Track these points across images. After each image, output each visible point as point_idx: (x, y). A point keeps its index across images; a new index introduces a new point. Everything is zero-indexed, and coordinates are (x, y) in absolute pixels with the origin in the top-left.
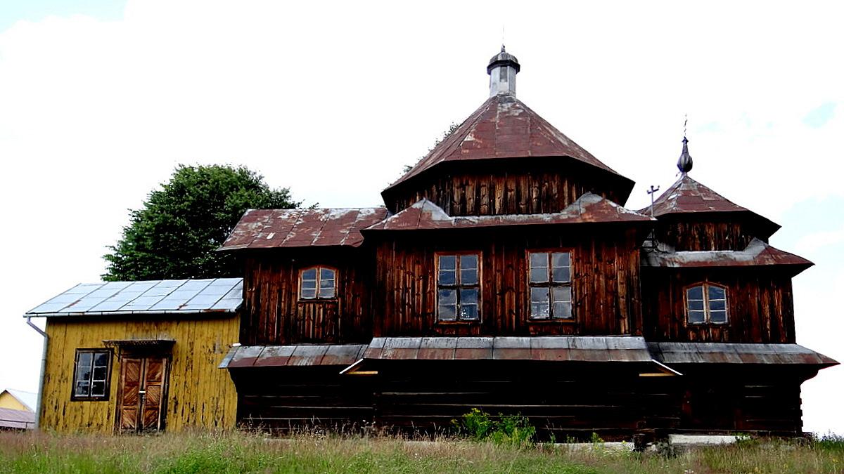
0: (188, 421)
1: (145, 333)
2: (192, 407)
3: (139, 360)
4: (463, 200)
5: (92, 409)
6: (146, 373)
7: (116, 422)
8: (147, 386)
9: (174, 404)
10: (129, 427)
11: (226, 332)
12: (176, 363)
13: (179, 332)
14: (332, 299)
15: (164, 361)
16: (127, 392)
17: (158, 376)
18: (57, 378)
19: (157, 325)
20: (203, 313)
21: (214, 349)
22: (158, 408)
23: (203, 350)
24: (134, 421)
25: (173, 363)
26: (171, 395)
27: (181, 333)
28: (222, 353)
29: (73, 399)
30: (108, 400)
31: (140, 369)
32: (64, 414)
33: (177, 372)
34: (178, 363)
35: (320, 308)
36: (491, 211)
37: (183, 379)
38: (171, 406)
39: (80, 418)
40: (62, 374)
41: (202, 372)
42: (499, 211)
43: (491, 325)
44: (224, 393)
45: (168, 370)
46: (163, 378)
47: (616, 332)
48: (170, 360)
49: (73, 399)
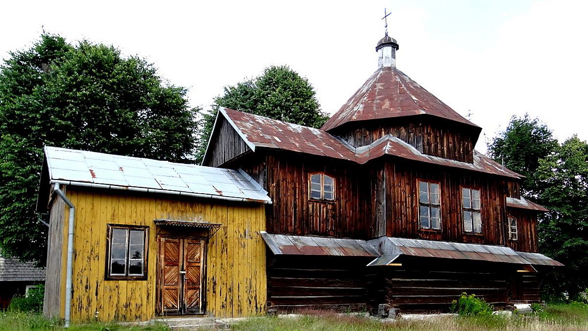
0: (226, 300)
1: (180, 215)
2: (228, 287)
3: (177, 240)
5: (129, 290)
6: (185, 254)
7: (156, 302)
8: (187, 267)
9: (212, 284)
10: (171, 306)
11: (253, 220)
12: (212, 246)
13: (213, 215)
14: (333, 201)
15: (202, 243)
16: (168, 272)
17: (197, 256)
18: (86, 255)
19: (192, 207)
20: (245, 201)
21: (245, 235)
22: (199, 288)
23: (235, 234)
24: (176, 301)
25: (209, 245)
27: (215, 218)
28: (252, 238)
29: (107, 278)
31: (179, 250)
32: (97, 294)
33: (214, 254)
34: (214, 245)
35: (323, 208)
36: (443, 157)
38: (210, 286)
40: (92, 251)
41: (236, 256)
44: (255, 275)
45: (206, 251)
46: (202, 259)
48: (207, 242)
49: (107, 278)
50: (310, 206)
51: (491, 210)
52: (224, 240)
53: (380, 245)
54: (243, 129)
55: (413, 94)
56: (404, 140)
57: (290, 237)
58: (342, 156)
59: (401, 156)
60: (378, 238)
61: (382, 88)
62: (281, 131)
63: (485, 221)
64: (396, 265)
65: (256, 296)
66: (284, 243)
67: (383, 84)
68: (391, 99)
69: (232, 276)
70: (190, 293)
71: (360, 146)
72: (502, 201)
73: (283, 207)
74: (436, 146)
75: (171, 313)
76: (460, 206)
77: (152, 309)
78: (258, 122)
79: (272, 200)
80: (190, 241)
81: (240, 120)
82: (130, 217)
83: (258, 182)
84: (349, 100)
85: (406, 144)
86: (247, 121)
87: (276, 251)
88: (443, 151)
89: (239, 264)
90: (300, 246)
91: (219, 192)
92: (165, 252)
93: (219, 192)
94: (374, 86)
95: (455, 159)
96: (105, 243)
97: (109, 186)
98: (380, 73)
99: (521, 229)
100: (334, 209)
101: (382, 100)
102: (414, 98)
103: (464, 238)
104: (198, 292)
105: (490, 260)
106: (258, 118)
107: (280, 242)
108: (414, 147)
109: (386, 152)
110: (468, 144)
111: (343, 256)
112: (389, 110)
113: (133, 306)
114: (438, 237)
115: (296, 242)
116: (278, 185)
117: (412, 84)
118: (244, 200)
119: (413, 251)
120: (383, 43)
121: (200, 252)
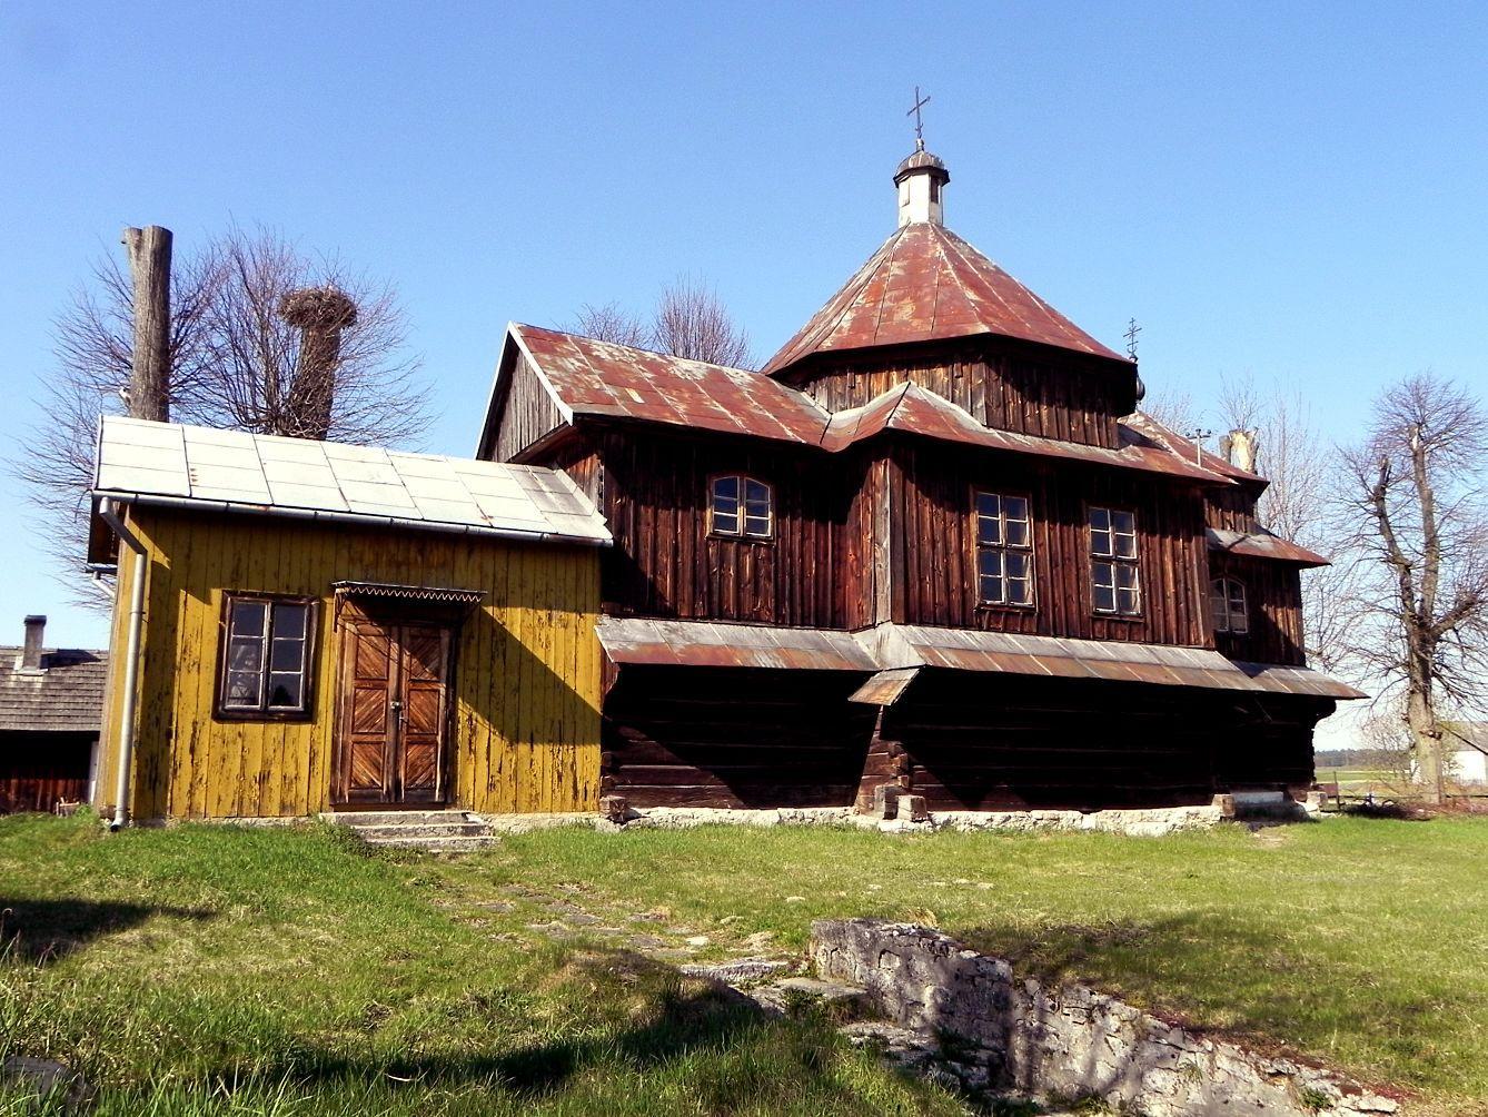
1: (394, 571)
11: (571, 583)
13: (473, 571)
14: (766, 539)
15: (445, 638)
28: (565, 627)
32: (192, 750)
33: (473, 663)
34: (474, 642)
37: (485, 677)
39: (239, 760)
42: (1049, 429)
47: (1184, 641)
48: (455, 637)
49: (220, 715)
53: (879, 646)
54: (555, 373)
56: (942, 394)
58: (790, 433)
59: (926, 432)
60: (874, 626)
61: (897, 272)
62: (650, 375)
65: (574, 762)
66: (639, 637)
67: (905, 263)
68: (916, 300)
70: (413, 752)
71: (842, 409)
75: (365, 799)
77: (321, 787)
78: (597, 356)
80: (414, 631)
82: (277, 575)
84: (829, 302)
85: (948, 403)
86: (572, 354)
91: (485, 518)
93: (485, 518)
94: (883, 269)
96: (215, 633)
97: (225, 504)
98: (901, 239)
101: (897, 299)
104: (432, 750)
106: (600, 348)
107: (632, 636)
108: (966, 410)
109: (890, 424)
111: (783, 670)
112: (909, 322)
113: (275, 781)
114: (1032, 624)
115: (673, 636)
117: (974, 262)
118: (545, 535)
119: (954, 658)
120: (911, 166)
121: (440, 656)
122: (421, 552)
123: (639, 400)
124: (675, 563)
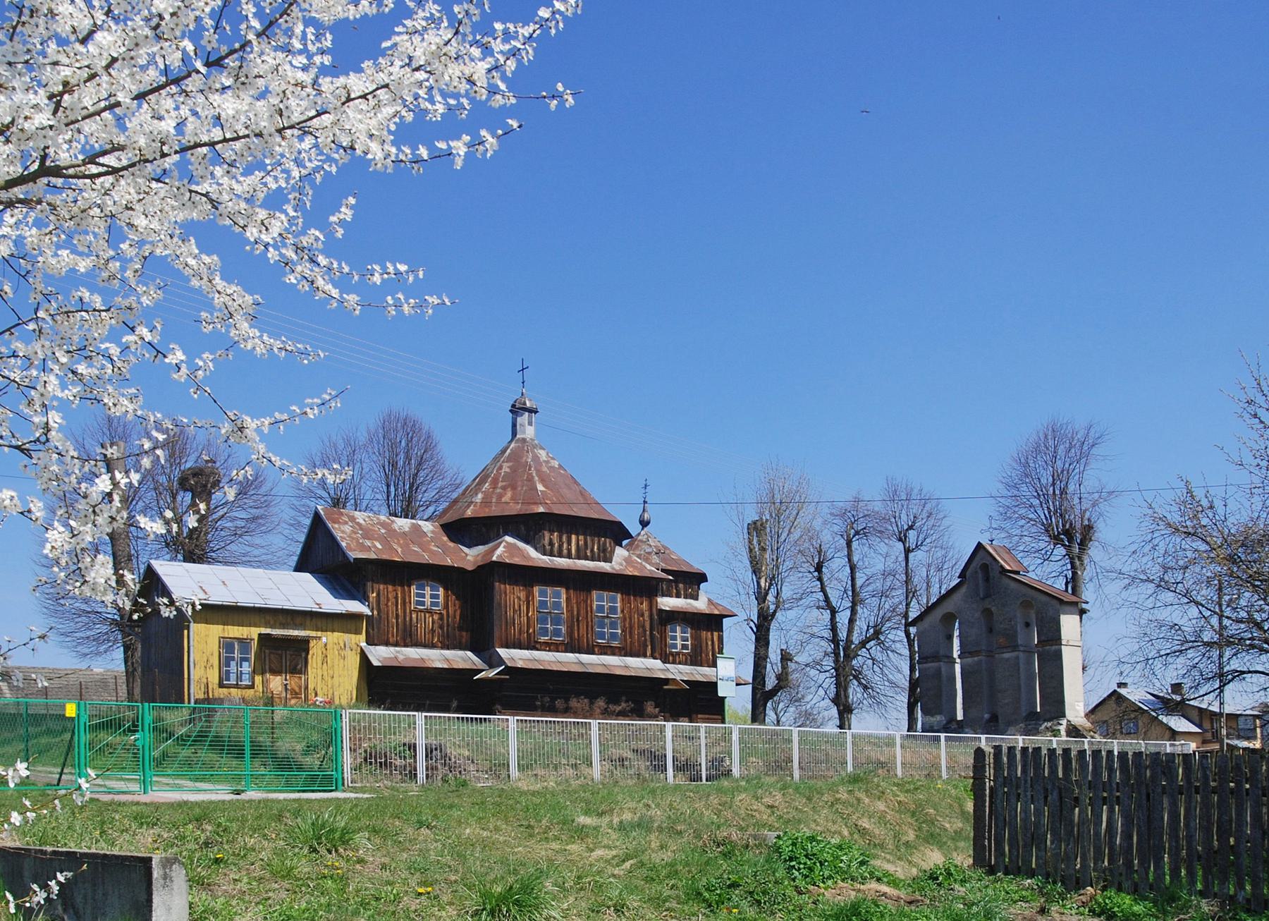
3: (280, 652)
4: (551, 544)
6: (288, 664)
17: (299, 667)
22: (301, 698)
26: (311, 686)
30: (254, 688)
33: (315, 666)
34: (315, 657)
36: (569, 556)
41: (336, 667)
43: (572, 646)
50: (414, 616)
51: (636, 616)
52: (324, 652)
55: (542, 481)
57: (392, 649)
61: (508, 470)
63: (628, 630)
64: (503, 677)
68: (514, 488)
69: (332, 687)
72: (652, 604)
73: (384, 616)
74: (561, 546)
76: (591, 612)
79: (372, 611)
81: (339, 523)
83: (358, 591)
86: (346, 523)
87: (376, 663)
88: (569, 550)
89: (340, 676)
90: (401, 657)
91: (318, 604)
92: (269, 662)
93: (318, 604)
95: (586, 558)
99: (696, 638)
100: (441, 618)
101: (504, 488)
102: (540, 487)
103: (596, 650)
105: (618, 673)
110: (605, 541)
116: (378, 595)
122: (292, 619)
123: (380, 547)
124: (397, 622)
